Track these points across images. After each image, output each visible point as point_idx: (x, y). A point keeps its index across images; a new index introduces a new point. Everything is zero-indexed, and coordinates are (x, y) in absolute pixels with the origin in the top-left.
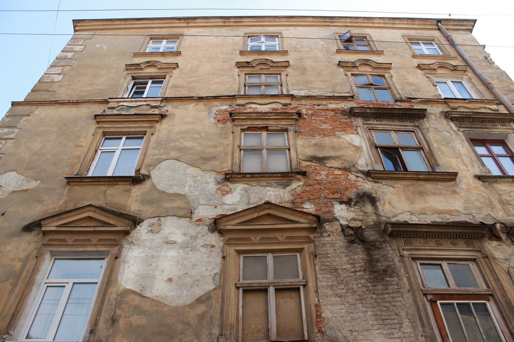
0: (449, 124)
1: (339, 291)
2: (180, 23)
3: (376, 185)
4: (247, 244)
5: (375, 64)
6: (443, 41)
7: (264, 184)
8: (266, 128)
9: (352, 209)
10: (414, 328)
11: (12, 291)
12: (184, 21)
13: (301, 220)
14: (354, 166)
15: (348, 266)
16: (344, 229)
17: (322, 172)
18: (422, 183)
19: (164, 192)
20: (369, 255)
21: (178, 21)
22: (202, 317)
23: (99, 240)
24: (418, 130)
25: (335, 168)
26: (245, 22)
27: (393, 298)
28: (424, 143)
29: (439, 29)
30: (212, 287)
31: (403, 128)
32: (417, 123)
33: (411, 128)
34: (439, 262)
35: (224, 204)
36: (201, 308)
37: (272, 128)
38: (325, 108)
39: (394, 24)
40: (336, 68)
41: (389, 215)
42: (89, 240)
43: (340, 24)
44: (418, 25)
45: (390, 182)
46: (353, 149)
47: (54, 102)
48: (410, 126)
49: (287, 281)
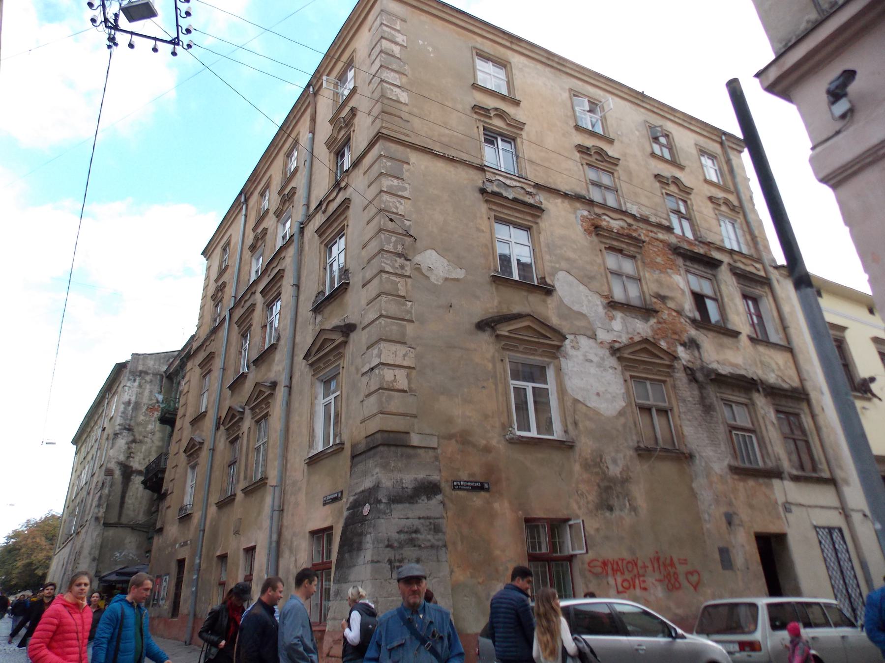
0: (732, 279)
1: (688, 417)
2: (503, 38)
3: (698, 332)
4: (637, 372)
5: (683, 186)
6: (722, 159)
7: (634, 316)
9: (688, 352)
11: (496, 390)
13: (665, 357)
15: (690, 399)
16: (686, 368)
17: (665, 311)
18: (721, 336)
19: (570, 309)
20: (701, 393)
22: (624, 426)
23: (543, 351)
24: (714, 279)
25: (672, 309)
28: (718, 294)
30: (624, 404)
32: (714, 272)
33: (709, 276)
34: (730, 403)
35: (613, 330)
36: (622, 420)
37: (626, 252)
38: (655, 236)
39: (690, 123)
40: (652, 178)
41: (708, 362)
42: (535, 350)
43: (648, 107)
44: (708, 132)
45: (705, 332)
46: (680, 292)
47: (428, 150)
49: (661, 404)
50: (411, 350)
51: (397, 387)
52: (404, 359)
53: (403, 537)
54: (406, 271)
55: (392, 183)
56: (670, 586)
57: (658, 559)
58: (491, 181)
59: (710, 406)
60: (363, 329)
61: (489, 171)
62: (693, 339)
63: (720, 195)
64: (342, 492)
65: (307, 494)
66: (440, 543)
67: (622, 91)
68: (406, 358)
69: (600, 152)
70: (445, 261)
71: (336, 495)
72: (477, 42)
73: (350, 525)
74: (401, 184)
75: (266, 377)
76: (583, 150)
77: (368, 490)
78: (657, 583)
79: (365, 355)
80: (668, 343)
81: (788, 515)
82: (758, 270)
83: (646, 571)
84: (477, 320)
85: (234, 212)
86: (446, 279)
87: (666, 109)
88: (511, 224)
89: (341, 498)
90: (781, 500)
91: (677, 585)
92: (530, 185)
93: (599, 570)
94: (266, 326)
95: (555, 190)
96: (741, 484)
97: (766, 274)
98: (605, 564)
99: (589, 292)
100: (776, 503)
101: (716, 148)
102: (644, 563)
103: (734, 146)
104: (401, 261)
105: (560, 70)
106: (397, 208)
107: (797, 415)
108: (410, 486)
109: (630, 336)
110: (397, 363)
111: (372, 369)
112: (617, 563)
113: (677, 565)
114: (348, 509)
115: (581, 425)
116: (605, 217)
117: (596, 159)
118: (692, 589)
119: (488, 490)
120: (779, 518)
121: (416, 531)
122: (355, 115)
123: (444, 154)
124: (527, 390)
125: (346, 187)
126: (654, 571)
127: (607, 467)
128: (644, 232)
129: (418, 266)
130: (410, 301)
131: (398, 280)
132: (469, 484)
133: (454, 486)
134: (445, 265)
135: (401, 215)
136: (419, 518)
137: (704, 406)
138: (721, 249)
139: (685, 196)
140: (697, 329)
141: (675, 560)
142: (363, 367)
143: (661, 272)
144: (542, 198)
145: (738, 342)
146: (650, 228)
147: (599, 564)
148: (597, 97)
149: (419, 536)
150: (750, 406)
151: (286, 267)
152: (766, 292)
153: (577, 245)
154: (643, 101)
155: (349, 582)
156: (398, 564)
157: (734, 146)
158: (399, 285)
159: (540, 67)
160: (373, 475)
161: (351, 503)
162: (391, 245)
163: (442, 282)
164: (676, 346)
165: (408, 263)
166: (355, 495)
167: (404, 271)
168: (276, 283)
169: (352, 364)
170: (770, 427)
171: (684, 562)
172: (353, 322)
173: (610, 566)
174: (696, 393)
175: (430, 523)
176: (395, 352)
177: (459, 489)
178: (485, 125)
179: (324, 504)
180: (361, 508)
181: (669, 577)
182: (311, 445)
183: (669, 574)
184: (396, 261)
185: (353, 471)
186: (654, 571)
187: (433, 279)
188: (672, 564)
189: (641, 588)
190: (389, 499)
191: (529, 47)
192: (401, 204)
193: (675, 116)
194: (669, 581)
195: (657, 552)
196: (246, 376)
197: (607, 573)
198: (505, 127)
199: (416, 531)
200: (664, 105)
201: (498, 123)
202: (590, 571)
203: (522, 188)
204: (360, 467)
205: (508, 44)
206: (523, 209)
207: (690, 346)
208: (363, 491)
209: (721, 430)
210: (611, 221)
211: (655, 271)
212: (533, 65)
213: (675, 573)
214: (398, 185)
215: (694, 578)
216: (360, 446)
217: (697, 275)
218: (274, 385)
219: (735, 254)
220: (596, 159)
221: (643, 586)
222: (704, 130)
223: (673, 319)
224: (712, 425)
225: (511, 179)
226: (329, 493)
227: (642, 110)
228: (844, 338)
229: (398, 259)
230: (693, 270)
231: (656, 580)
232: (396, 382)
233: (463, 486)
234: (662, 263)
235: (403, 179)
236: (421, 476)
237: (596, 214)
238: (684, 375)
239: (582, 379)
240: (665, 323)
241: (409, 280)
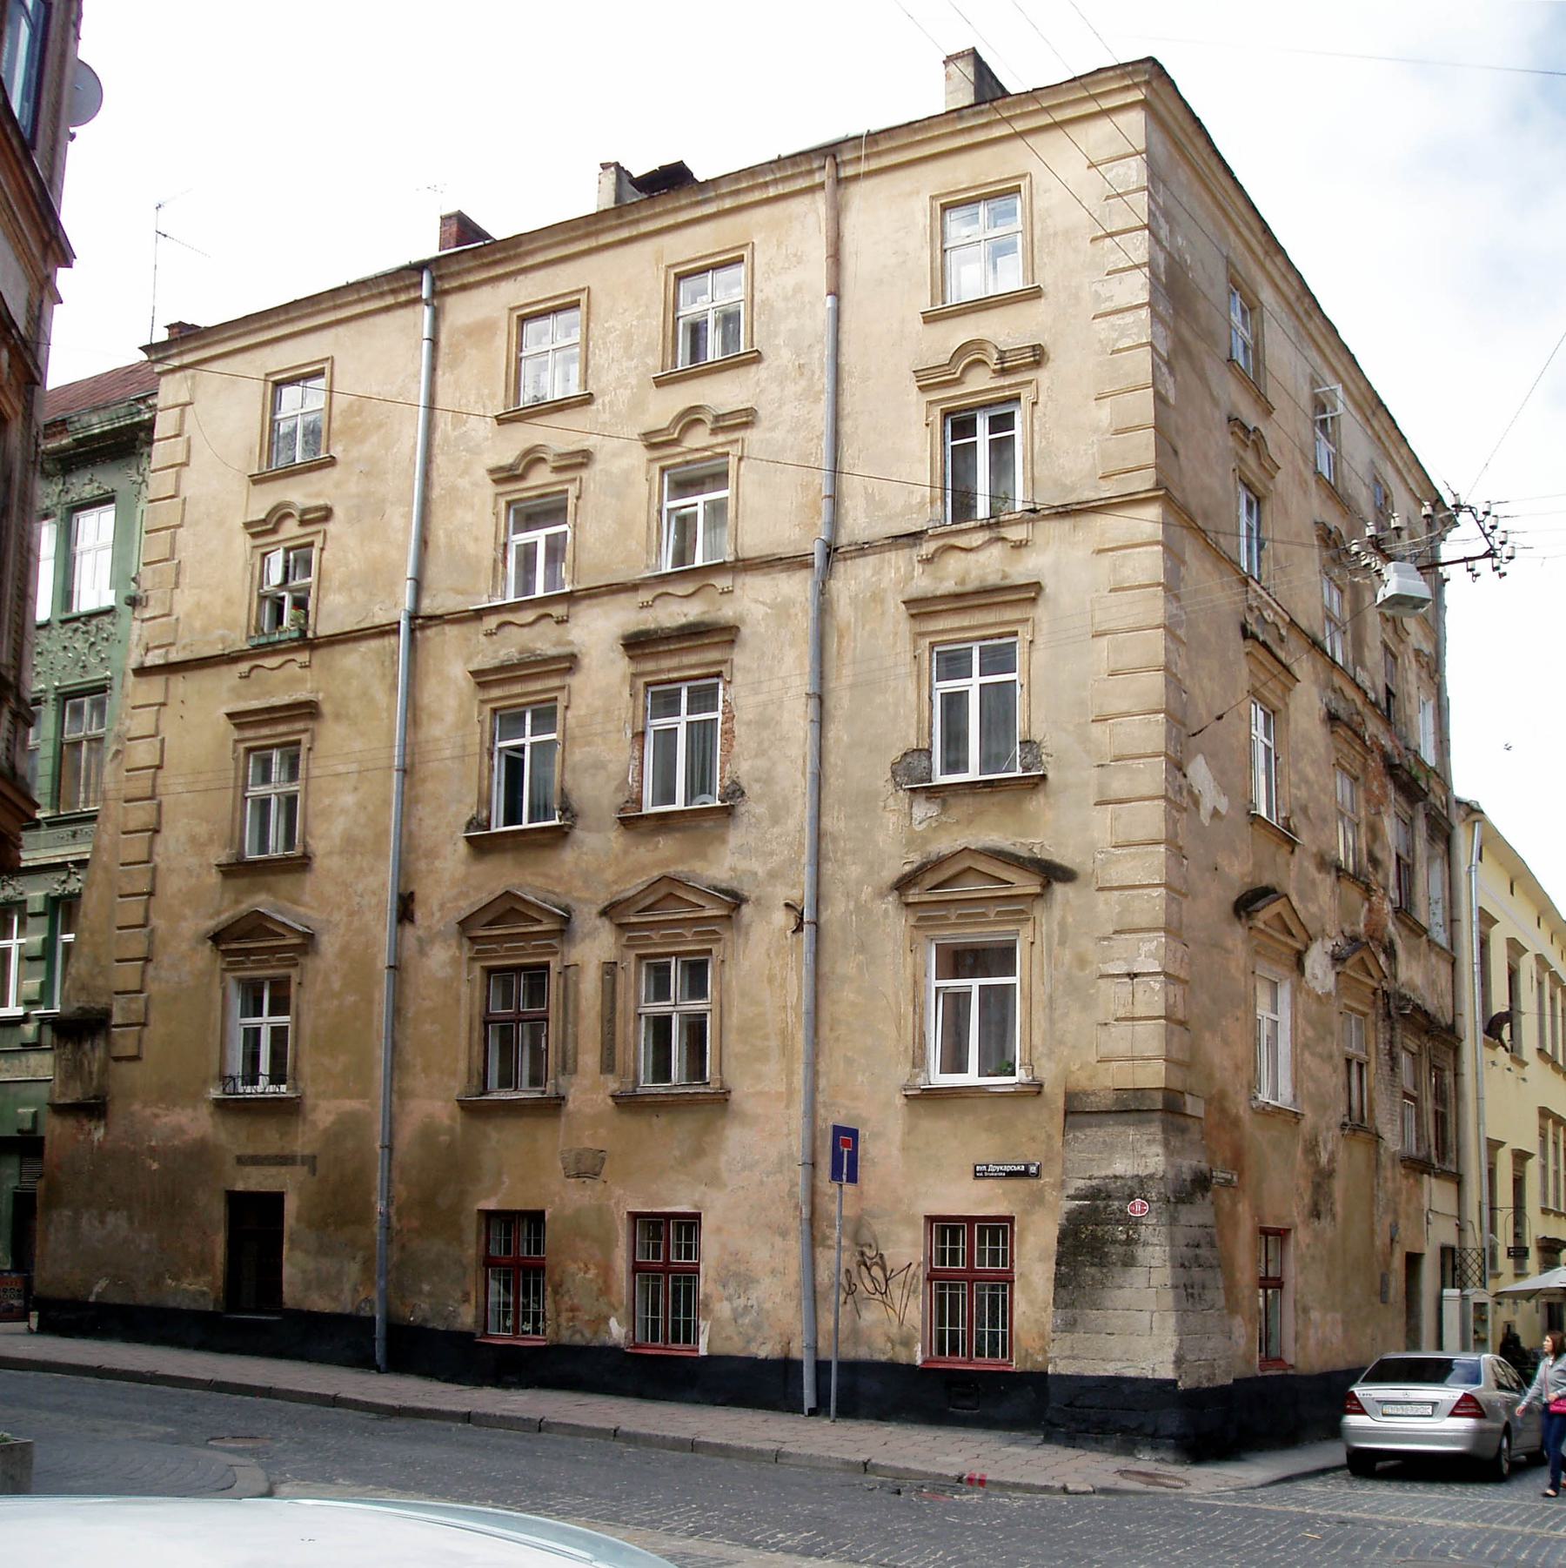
60: (1101, 889)
65: (905, 1149)
66: (1215, 1262)
79: (1112, 943)
85: (362, 300)
89: (1037, 1175)
94: (643, 734)
107: (1442, 1070)
108: (1189, 1179)
111: (1136, 975)
166: (1090, 1178)
179: (977, 1175)
182: (919, 1062)
196: (567, 833)
218: (735, 900)
226: (990, 1160)
236: (1195, 1163)
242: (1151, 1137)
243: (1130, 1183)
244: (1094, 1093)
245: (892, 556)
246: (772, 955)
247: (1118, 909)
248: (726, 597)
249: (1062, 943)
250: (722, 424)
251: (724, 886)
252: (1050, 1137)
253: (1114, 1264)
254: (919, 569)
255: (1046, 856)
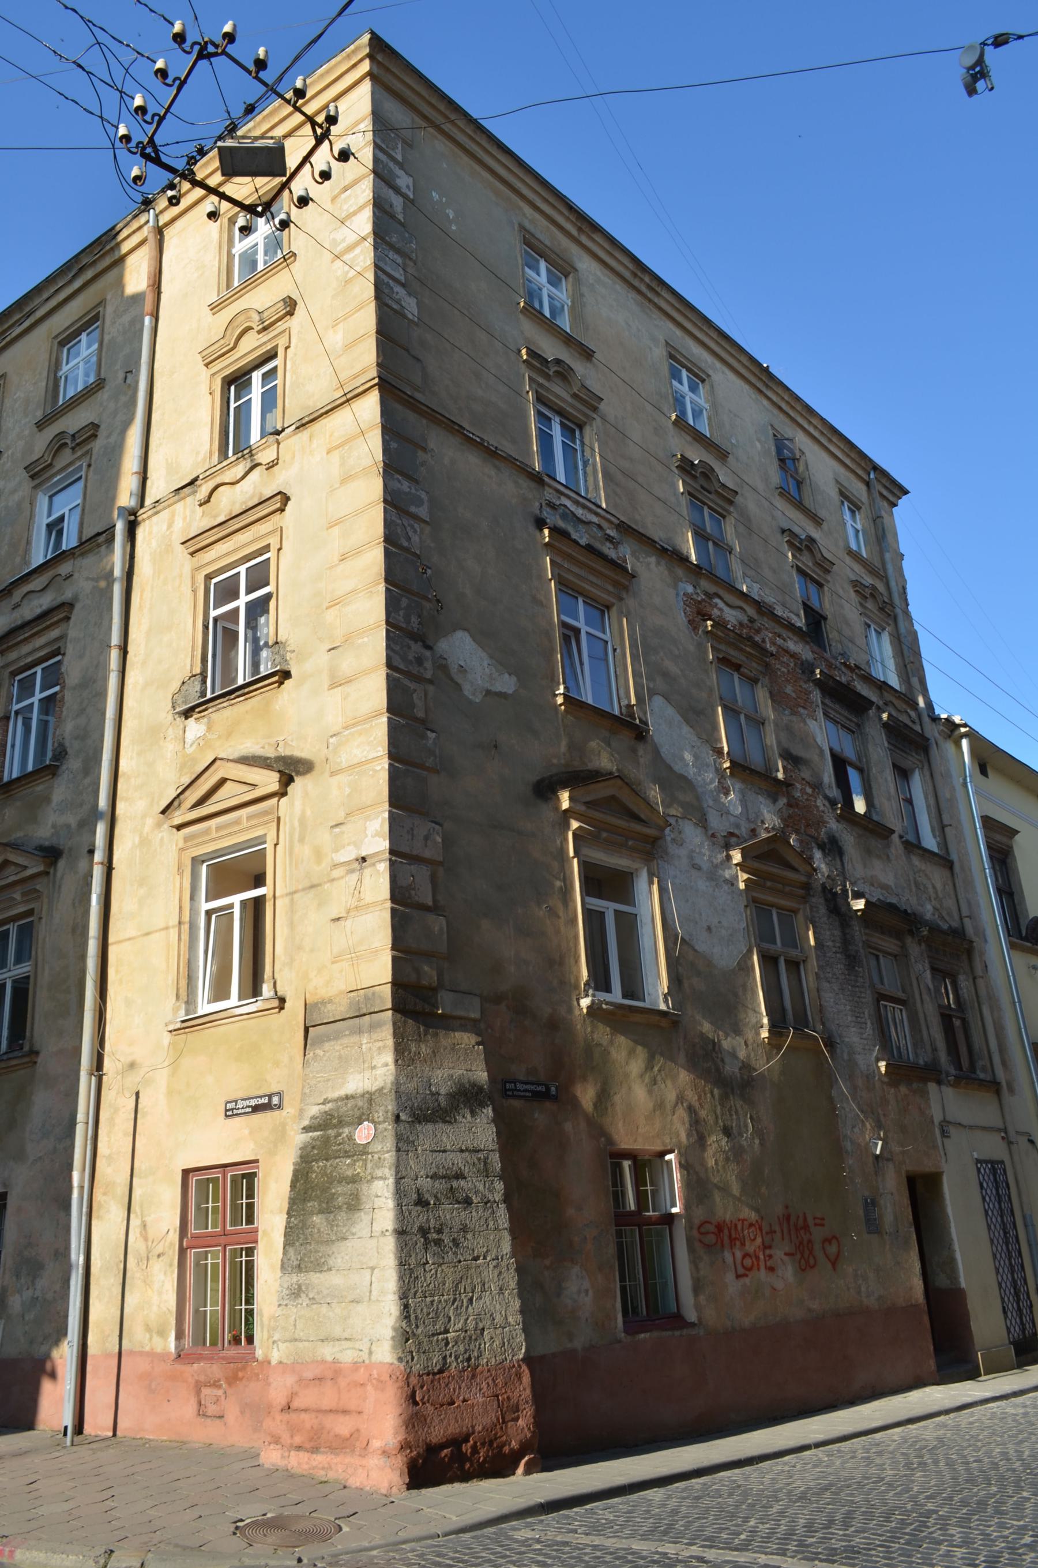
2: (568, 219)
5: (820, 555)
8: (737, 667)
10: (873, 1030)
12: (577, 219)
14: (821, 784)
15: (830, 943)
20: (844, 934)
21: (566, 212)
26: (663, 298)
27: (861, 992)
29: (868, 484)
31: (848, 723)
33: (853, 726)
37: (746, 671)
39: (830, 440)
43: (774, 398)
44: (853, 460)
47: (457, 427)
48: (853, 722)
50: (437, 827)
51: (417, 898)
52: (426, 846)
53: (440, 1185)
54: (426, 669)
55: (399, 486)
56: (803, 1262)
57: (788, 1218)
58: (552, 506)
59: (855, 957)
61: (550, 486)
62: (834, 837)
63: (868, 580)
64: (279, 1094)
65: (170, 1093)
67: (740, 361)
68: (429, 842)
69: (707, 473)
70: (484, 655)
71: (265, 1100)
72: (524, 215)
73: (317, 1161)
74: (413, 491)
75: (20, 834)
76: (686, 467)
77: (363, 1096)
78: (786, 1258)
79: (343, 828)
80: (801, 842)
81: (946, 1140)
82: (914, 722)
83: (773, 1240)
84: (534, 778)
86: (488, 693)
87: (799, 408)
88: (581, 594)
89: (279, 1107)
90: (937, 1118)
91: (812, 1262)
92: (611, 523)
93: (711, 1239)
95: (649, 538)
96: (892, 1090)
97: (922, 729)
98: (720, 1228)
99: (696, 739)
100: (933, 1122)
101: (858, 489)
102: (771, 1225)
103: (885, 493)
104: (416, 647)
105: (650, 301)
106: (409, 539)
108: (443, 1091)
109: (753, 826)
110: (415, 853)
112: (736, 1225)
113: (812, 1229)
114: (306, 1129)
115: (686, 984)
116: (717, 600)
117: (702, 487)
118: (829, 1266)
119: (555, 1099)
120: (935, 1147)
121: (459, 1176)
122: (291, 313)
123: (482, 439)
124: (606, 915)
125: (272, 465)
126: (783, 1239)
127: (723, 1060)
128: (770, 635)
129: (444, 662)
130: (433, 731)
131: (412, 686)
132: (528, 1087)
133: (506, 1090)
134: (485, 663)
135: (415, 554)
136: (462, 1151)
137: (848, 956)
138: (869, 679)
139: (821, 574)
140: (838, 821)
141: (810, 1221)
142: (336, 851)
143: (794, 713)
144: (627, 553)
145: (888, 846)
146: (779, 630)
147: (711, 1228)
148: (703, 365)
149: (462, 1183)
150: (901, 958)
151: (76, 598)
152: (920, 761)
153: (678, 649)
154: (767, 386)
155: (330, 1269)
156: (435, 1236)
157: (885, 493)
158: (415, 696)
159: (620, 287)
160: (373, 1068)
161: (313, 1118)
162: (401, 613)
163: (480, 697)
164: (811, 849)
165: (428, 653)
166: (323, 1104)
167: (422, 671)
168: (47, 628)
169: (302, 840)
170: (926, 997)
171: (820, 1223)
172: (298, 753)
173: (726, 1232)
174: (837, 933)
175: (479, 1159)
176: (412, 829)
177: (514, 1097)
178: (539, 390)
180: (346, 1131)
181: (801, 1248)
183: (801, 1243)
184: (409, 648)
185: (310, 1055)
186: (783, 1239)
187: (467, 690)
188: (806, 1227)
189: (766, 1268)
190: (413, 1115)
191: (607, 245)
192: (415, 532)
193: (810, 423)
194: (802, 1256)
195: (787, 1207)
197: (723, 1246)
198: (570, 399)
199: (459, 1176)
200: (798, 399)
201: (558, 391)
202: (700, 1241)
203: (599, 527)
204: (333, 1049)
205: (574, 232)
206: (603, 570)
207: (829, 850)
208: (347, 1097)
209: (868, 997)
210: (726, 609)
211: (784, 709)
212: (610, 282)
213: (810, 1241)
214: (409, 493)
215: (833, 1249)
216: (329, 1007)
217: (838, 723)
219: (887, 691)
220: (702, 487)
221: (768, 1264)
222: (848, 456)
223: (807, 800)
224: (857, 989)
225: (584, 507)
227: (765, 402)
228: (1011, 847)
229: (412, 643)
230: (832, 714)
231: (786, 1254)
232: (414, 889)
233: (520, 1090)
234: (794, 695)
235: (417, 482)
236: (458, 1072)
237: (706, 593)
238: (822, 901)
239: (687, 901)
240: (797, 805)
241: (431, 688)
242: (381, 1044)
243: (360, 1104)
244: (330, 1001)
245: (179, 507)
246: (77, 905)
247: (347, 791)
248: (67, 582)
249: (302, 840)
250: (78, 441)
251: (47, 843)
252: (291, 1059)
253: (340, 1208)
254: (199, 510)
255: (288, 752)
